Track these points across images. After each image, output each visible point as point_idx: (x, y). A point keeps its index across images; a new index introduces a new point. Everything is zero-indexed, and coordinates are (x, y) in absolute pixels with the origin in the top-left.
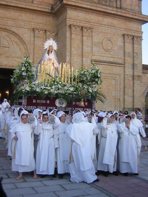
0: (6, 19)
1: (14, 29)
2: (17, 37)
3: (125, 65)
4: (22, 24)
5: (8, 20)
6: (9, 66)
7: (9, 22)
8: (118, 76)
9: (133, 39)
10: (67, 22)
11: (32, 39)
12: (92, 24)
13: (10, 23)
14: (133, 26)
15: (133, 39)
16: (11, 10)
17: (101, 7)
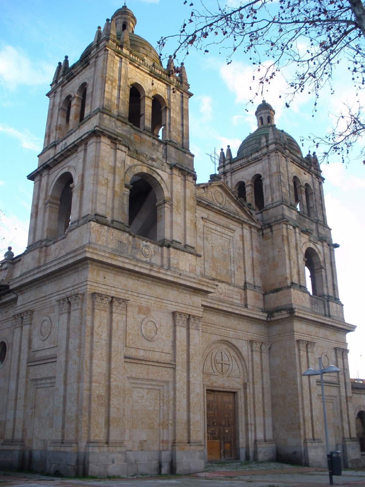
0: (228, 329)
1: (234, 342)
2: (235, 351)
3: (339, 384)
4: (241, 335)
5: (230, 330)
6: (231, 389)
7: (231, 332)
8: (334, 398)
9: (188, 320)
10: (295, 336)
11: (250, 353)
12: (313, 337)
13: (231, 333)
14: (339, 335)
15: (188, 320)
16: (231, 317)
17: (321, 318)
